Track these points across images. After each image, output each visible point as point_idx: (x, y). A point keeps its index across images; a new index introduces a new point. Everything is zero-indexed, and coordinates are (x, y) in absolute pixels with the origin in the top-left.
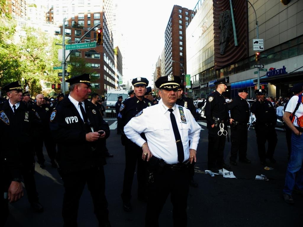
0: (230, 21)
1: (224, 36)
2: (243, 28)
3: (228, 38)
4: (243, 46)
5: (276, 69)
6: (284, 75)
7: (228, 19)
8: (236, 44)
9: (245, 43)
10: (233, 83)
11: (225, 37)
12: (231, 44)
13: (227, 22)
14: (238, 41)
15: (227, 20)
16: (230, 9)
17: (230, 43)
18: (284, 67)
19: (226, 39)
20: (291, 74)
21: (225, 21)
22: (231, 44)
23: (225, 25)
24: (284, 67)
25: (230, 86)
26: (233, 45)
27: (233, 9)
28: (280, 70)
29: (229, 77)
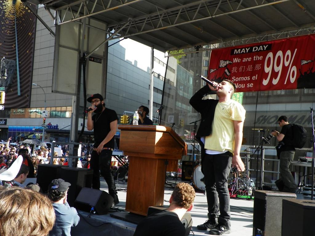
0: (14, 70)
1: (6, 82)
2: (27, 83)
3: (10, 84)
4: (26, 97)
5: (52, 125)
6: (57, 130)
7: (13, 68)
8: (19, 94)
9: (28, 96)
10: (11, 125)
11: (7, 83)
12: (13, 91)
13: (11, 70)
14: (21, 91)
15: (11, 68)
16: (15, 60)
17: (11, 90)
18: (57, 125)
19: (8, 85)
20: (61, 130)
21: (10, 69)
22: (13, 91)
23: (9, 72)
24: (57, 125)
25: (8, 128)
26: (15, 92)
27: (19, 61)
28: (55, 126)
29: (6, 120)
